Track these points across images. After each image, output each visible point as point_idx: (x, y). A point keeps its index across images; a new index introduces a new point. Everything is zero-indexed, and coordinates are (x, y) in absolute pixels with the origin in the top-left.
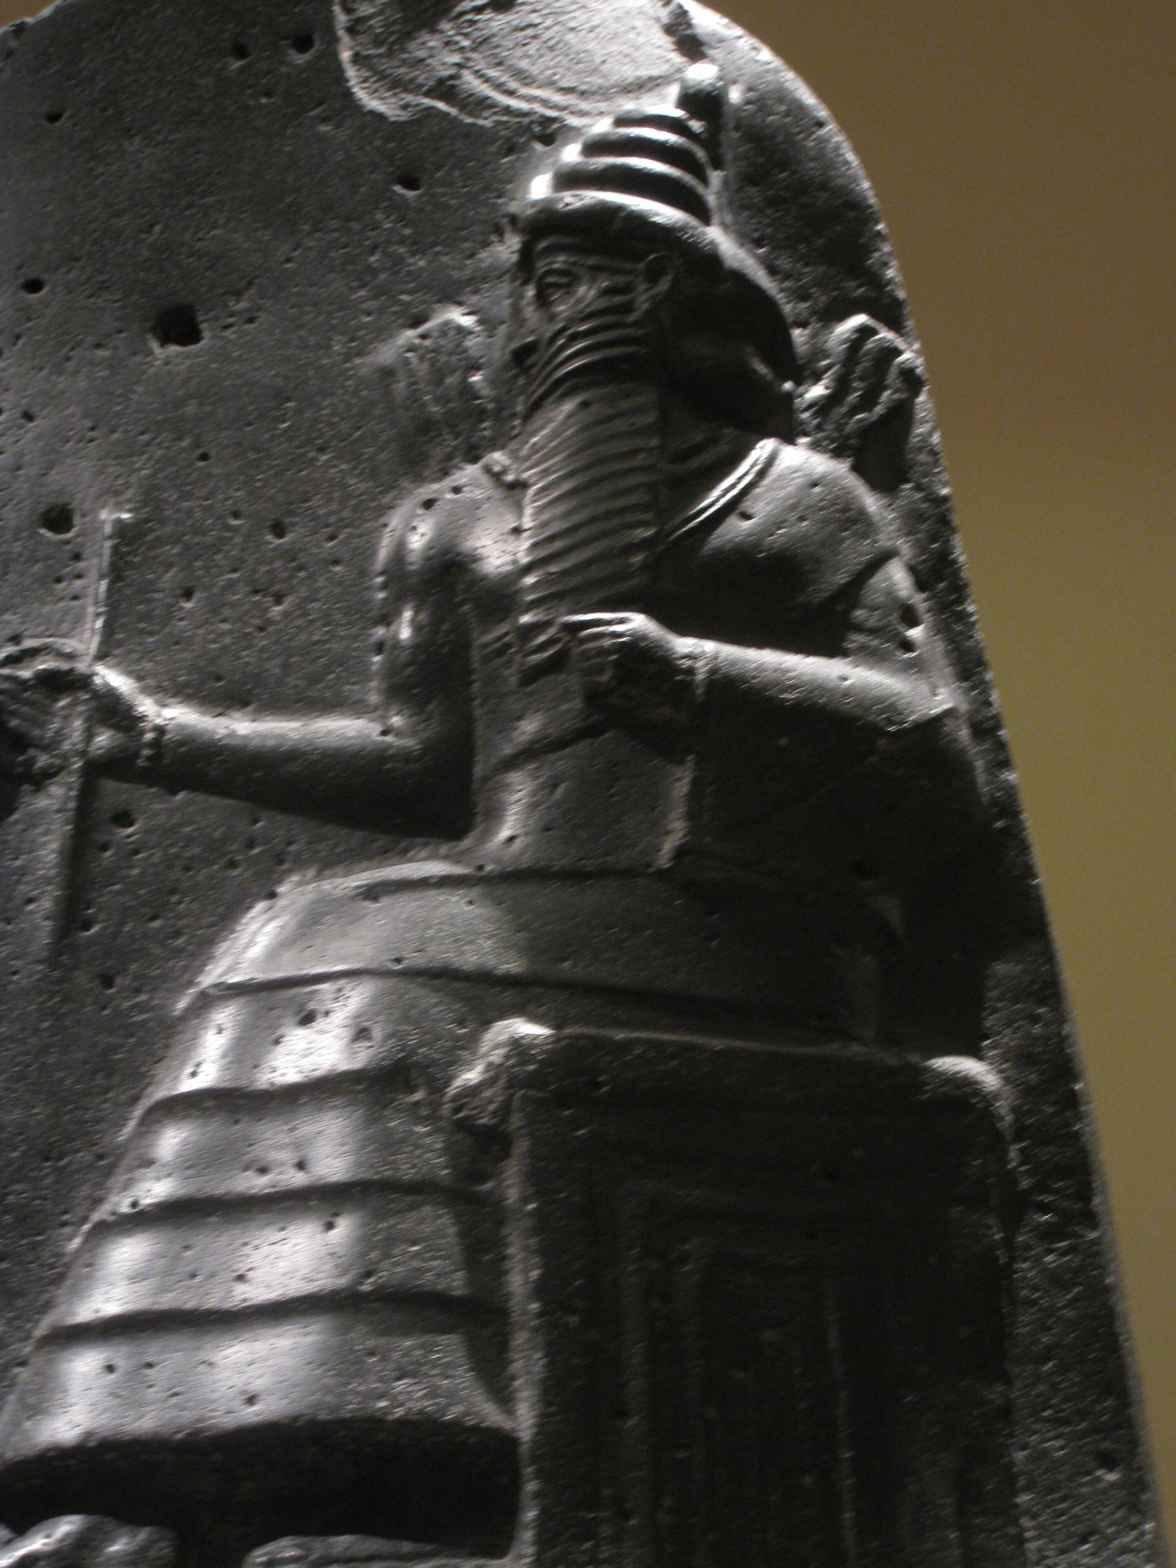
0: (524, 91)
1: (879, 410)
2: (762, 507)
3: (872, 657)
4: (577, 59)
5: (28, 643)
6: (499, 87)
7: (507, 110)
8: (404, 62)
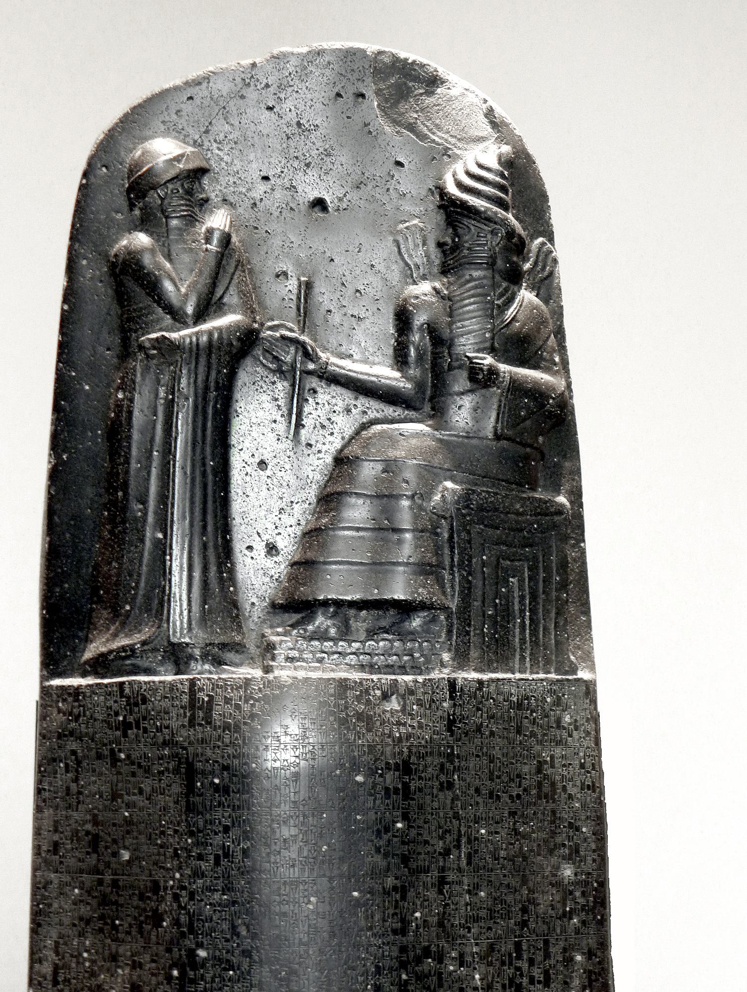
0: (439, 134)
1: (546, 273)
2: (519, 317)
3: (547, 370)
4: (456, 123)
5: (276, 323)
6: (430, 130)
7: (433, 141)
8: (396, 113)
